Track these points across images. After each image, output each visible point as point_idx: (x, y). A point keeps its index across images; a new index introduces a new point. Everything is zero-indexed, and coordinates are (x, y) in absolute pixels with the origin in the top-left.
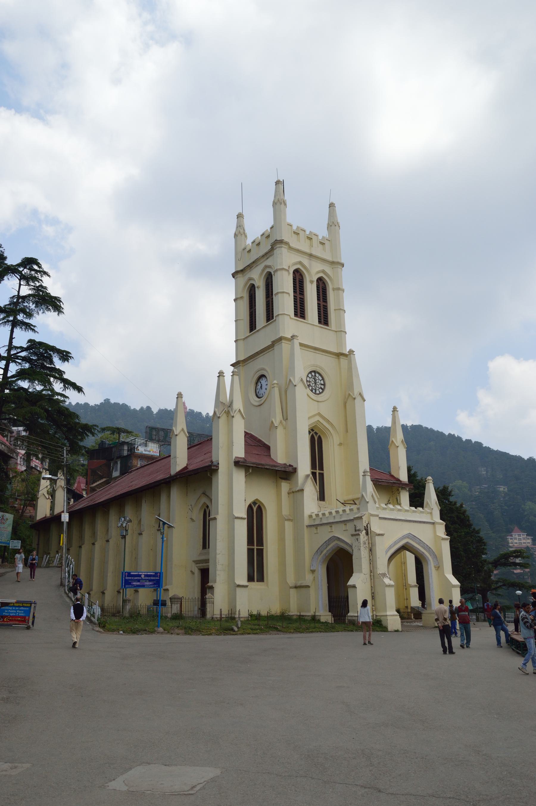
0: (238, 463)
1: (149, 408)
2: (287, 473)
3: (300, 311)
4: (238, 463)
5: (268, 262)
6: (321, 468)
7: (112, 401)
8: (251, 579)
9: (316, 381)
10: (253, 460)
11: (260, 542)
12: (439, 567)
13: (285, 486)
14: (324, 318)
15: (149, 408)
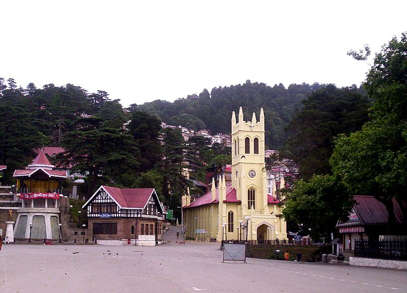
0: (224, 202)
1: (281, 85)
2: (239, 203)
3: (247, 151)
4: (224, 202)
5: (238, 135)
6: (254, 200)
7: (252, 82)
8: (229, 231)
9: (252, 174)
10: (228, 201)
11: (232, 222)
12: (274, 230)
13: (239, 206)
14: (256, 151)
15: (281, 85)
